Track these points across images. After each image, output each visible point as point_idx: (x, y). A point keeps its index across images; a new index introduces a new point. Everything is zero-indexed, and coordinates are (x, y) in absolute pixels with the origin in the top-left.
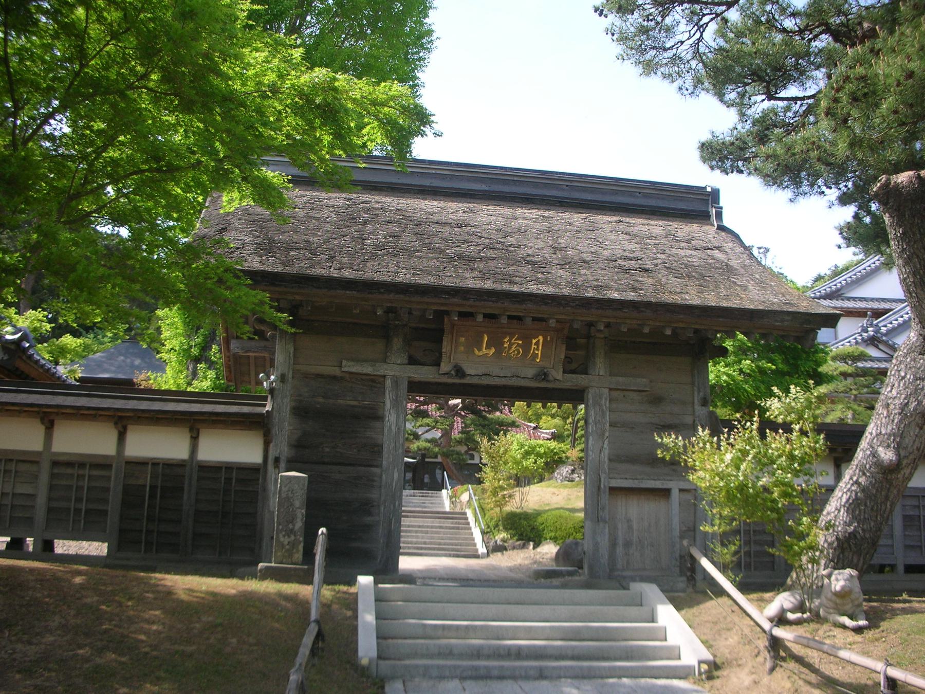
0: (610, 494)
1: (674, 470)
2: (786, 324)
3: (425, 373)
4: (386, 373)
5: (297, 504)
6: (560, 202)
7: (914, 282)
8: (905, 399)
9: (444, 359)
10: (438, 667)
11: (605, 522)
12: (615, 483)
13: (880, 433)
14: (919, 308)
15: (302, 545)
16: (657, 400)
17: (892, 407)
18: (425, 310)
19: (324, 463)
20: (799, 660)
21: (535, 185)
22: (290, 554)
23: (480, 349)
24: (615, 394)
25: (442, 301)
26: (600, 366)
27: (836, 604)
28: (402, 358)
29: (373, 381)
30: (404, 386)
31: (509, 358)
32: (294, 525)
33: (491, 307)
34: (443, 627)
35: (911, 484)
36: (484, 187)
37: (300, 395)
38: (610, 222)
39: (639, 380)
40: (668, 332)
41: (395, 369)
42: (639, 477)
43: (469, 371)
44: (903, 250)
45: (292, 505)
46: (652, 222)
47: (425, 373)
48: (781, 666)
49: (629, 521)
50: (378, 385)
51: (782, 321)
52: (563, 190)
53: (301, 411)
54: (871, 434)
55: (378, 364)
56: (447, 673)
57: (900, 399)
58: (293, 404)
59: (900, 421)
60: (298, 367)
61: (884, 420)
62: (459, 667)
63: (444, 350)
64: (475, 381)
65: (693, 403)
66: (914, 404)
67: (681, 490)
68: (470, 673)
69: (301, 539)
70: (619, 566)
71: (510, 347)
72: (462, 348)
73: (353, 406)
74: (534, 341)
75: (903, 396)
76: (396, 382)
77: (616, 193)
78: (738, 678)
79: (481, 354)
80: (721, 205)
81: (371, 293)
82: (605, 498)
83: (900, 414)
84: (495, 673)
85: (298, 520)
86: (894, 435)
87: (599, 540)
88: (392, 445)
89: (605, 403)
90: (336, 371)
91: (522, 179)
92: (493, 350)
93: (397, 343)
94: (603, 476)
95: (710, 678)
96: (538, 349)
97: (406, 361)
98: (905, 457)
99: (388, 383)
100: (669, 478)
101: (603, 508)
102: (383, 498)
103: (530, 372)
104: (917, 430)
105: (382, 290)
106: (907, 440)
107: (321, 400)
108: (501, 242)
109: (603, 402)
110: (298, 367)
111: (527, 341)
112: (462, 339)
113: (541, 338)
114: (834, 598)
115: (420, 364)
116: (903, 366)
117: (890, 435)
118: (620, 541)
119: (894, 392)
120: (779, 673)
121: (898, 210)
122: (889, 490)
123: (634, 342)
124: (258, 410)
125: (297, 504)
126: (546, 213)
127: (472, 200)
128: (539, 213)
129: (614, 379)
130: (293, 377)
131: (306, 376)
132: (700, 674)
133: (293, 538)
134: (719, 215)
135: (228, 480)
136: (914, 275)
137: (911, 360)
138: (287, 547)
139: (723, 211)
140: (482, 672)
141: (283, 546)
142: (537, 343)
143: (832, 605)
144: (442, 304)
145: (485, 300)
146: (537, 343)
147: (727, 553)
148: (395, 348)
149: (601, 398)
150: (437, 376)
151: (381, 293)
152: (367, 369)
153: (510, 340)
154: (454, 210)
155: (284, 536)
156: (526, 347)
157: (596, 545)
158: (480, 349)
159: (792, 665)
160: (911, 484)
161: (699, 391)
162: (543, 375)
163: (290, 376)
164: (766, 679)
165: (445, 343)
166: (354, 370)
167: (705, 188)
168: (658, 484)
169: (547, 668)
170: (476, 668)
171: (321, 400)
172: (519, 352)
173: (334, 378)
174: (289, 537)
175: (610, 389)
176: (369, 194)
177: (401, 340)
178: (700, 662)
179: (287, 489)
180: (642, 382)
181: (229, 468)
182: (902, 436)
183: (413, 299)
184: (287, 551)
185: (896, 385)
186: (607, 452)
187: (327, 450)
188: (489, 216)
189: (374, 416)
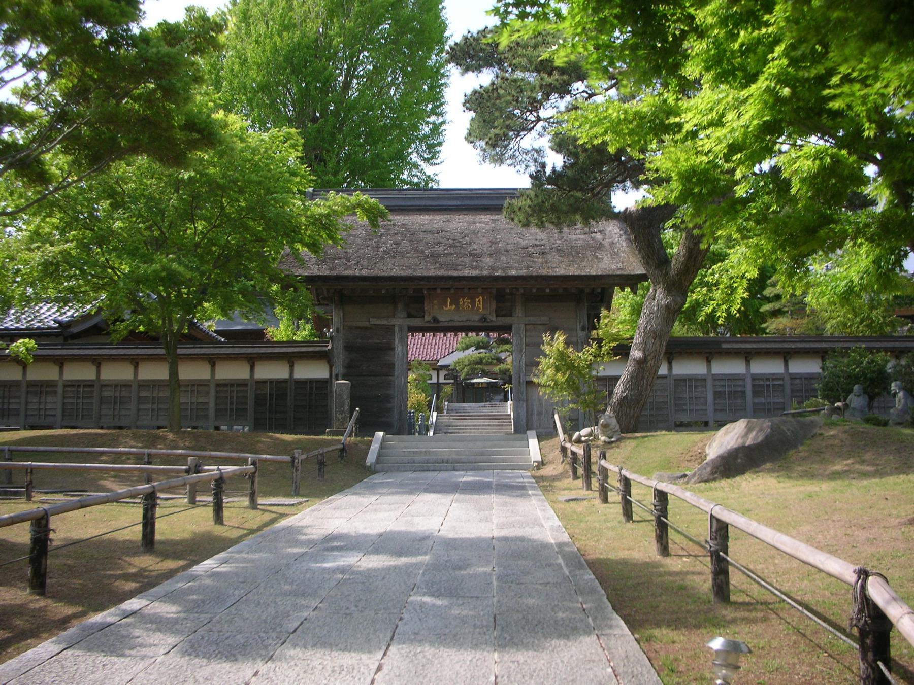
3: (416, 322)
5: (345, 397)
26: (519, 311)
36: (459, 203)
41: (399, 321)
47: (416, 322)
53: (349, 348)
64: (446, 324)
76: (401, 329)
90: (367, 324)
92: (454, 307)
93: (400, 306)
99: (396, 329)
103: (477, 318)
125: (345, 397)
126: (495, 217)
129: (528, 318)
135: (311, 388)
152: (384, 322)
162: (484, 319)
173: (366, 328)
180: (544, 319)
181: (311, 381)
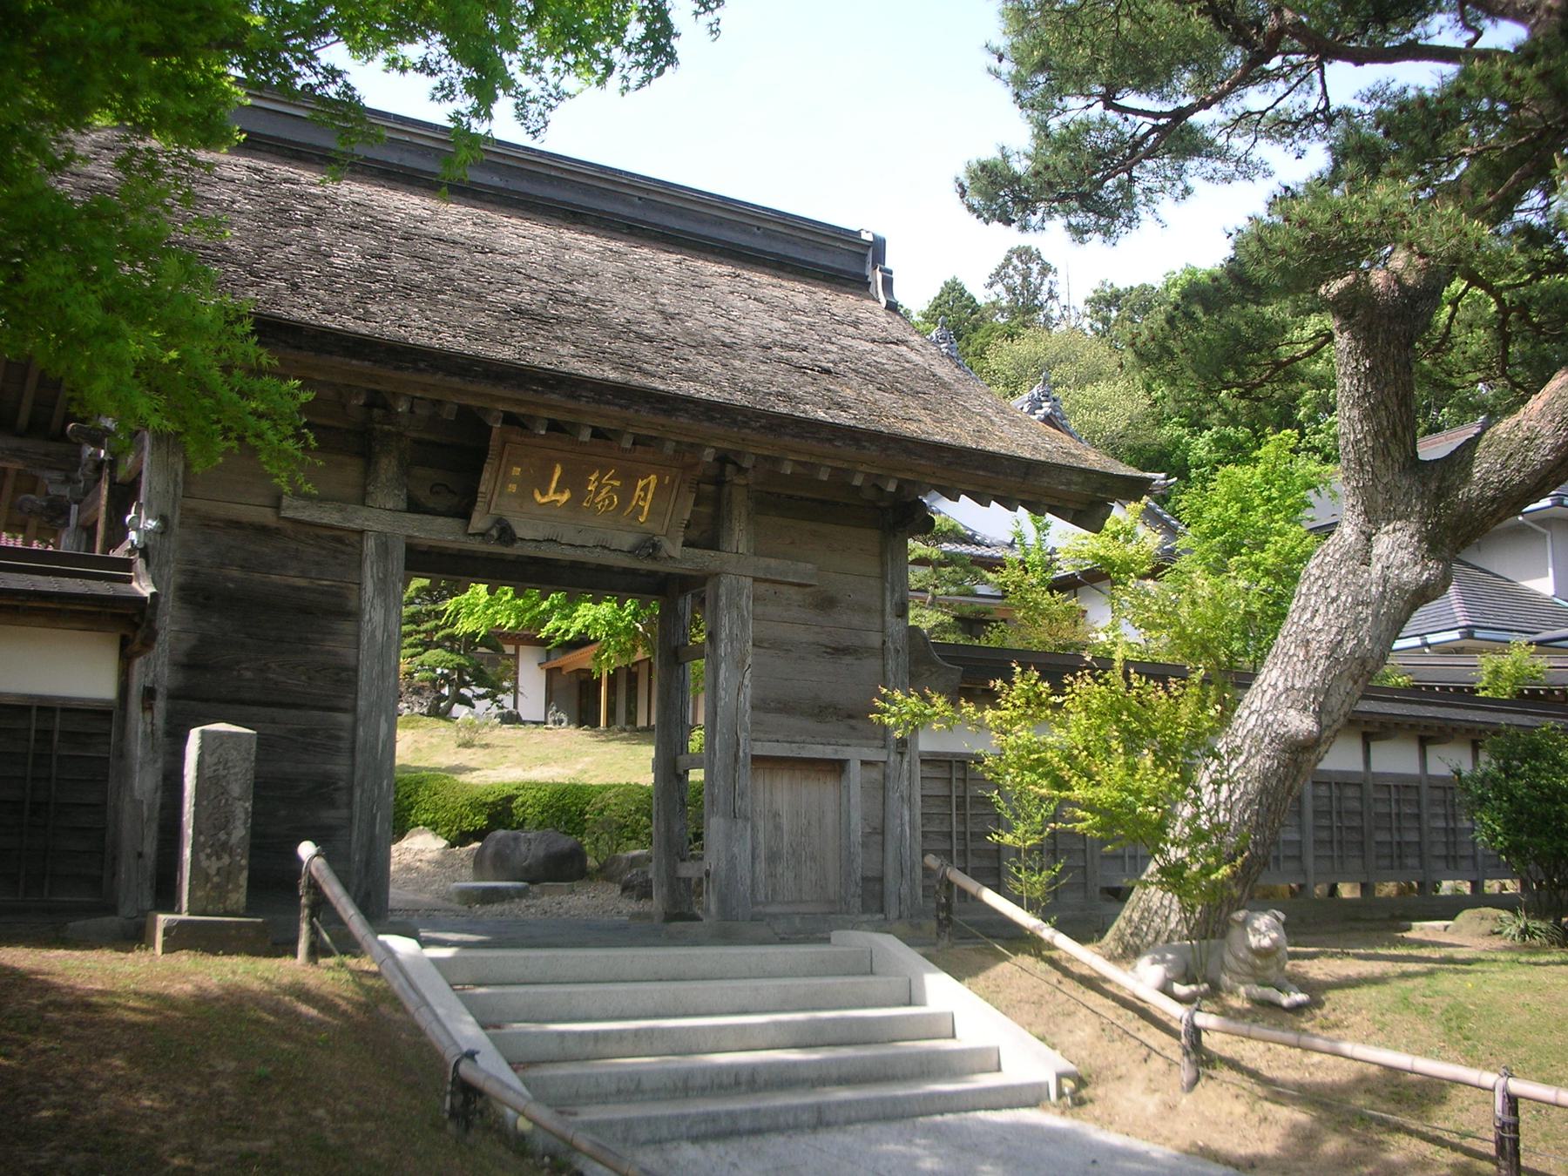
0: (754, 770)
1: (853, 728)
2: (1074, 488)
3: (439, 531)
4: (367, 525)
5: (236, 790)
6: (629, 227)
7: (1372, 448)
8: (1338, 633)
9: (480, 505)
10: (649, 1121)
11: (746, 818)
12: (763, 749)
13: (1293, 687)
14: (1371, 490)
15: (245, 874)
16: (826, 603)
17: (1314, 645)
18: (438, 403)
19: (243, 702)
20: (1234, 1065)
21: (587, 190)
22: (221, 891)
23: (544, 493)
24: (763, 587)
25: (529, 396)
26: (739, 537)
27: (1253, 966)
28: (396, 500)
29: (340, 540)
30: (399, 553)
31: (593, 508)
32: (229, 834)
33: (610, 415)
34: (596, 1034)
35: (1321, 766)
36: (495, 181)
37: (194, 562)
38: (721, 275)
39: (802, 565)
40: (891, 487)
41: (384, 520)
42: (798, 738)
43: (520, 533)
44: (1366, 394)
45: (225, 792)
46: (785, 283)
47: (439, 531)
48: (1211, 1077)
49: (776, 815)
50: (349, 549)
51: (1069, 483)
52: (633, 205)
53: (197, 594)
54: (1275, 686)
55: (350, 508)
56: (665, 1133)
57: (1329, 633)
58: (181, 579)
59: (1327, 670)
60: (191, 503)
61: (1299, 666)
62: (684, 1117)
63: (482, 489)
64: (530, 550)
65: (883, 611)
66: (1352, 643)
67: (863, 763)
68: (703, 1127)
69: (244, 862)
70: (761, 897)
71: (598, 492)
72: (513, 488)
73: (299, 588)
74: (641, 483)
75: (1334, 630)
76: (384, 549)
77: (720, 222)
78: (1128, 1100)
79: (545, 500)
80: (888, 265)
81: (397, 368)
82: (745, 775)
83: (1328, 658)
84: (746, 1123)
85: (238, 823)
86: (1316, 690)
87: (736, 850)
88: (377, 668)
89: (746, 603)
90: (267, 516)
91: (564, 176)
92: (566, 497)
93: (387, 467)
94: (742, 736)
95: (1080, 1102)
96: (644, 499)
97: (403, 505)
98: (1329, 727)
99: (370, 545)
100: (843, 741)
101: (742, 795)
102: (359, 774)
103: (627, 540)
104: (1351, 683)
105: (422, 365)
106: (1333, 700)
107: (236, 573)
108: (567, 292)
109: (743, 602)
110: (191, 503)
111: (629, 479)
112: (517, 471)
113: (653, 477)
114: (1250, 957)
115: (425, 513)
116: (1333, 581)
117: (1309, 691)
118: (762, 852)
119: (1318, 622)
120: (1206, 1089)
121: (1368, 329)
122: (1295, 780)
123: (791, 497)
124: (120, 589)
125: (236, 790)
126: (613, 245)
127: (478, 204)
128: (602, 242)
129: (764, 562)
130: (181, 524)
131: (207, 523)
132: (1060, 1095)
133: (226, 860)
134: (888, 284)
135: (45, 735)
136: (1376, 436)
137: (1348, 572)
138: (216, 879)
139: (894, 276)
140: (724, 1124)
141: (208, 878)
142: (645, 489)
143: (1246, 968)
144: (519, 402)
145: (608, 403)
146: (645, 489)
147: (1036, 882)
148: (383, 478)
149: (740, 595)
150: (462, 539)
151: (420, 371)
152: (330, 516)
153: (599, 479)
154: (455, 219)
155: (209, 857)
156: (626, 493)
157: (732, 860)
158: (544, 493)
159: (1226, 1074)
160: (1321, 766)
161: (893, 591)
162: (649, 547)
163: (176, 521)
164: (1185, 1100)
165: (486, 476)
166: (305, 515)
167: (859, 233)
168: (828, 752)
169: (829, 1105)
170: (713, 1118)
171: (236, 573)
172: (612, 502)
173: (262, 530)
174: (219, 858)
175: (755, 580)
176: (289, 164)
177: (394, 462)
178: (1060, 1077)
179: (214, 759)
180: (804, 570)
181: (46, 708)
182: (1327, 693)
183: (472, 388)
184: (217, 887)
185: (1322, 610)
186: (749, 691)
187: (248, 674)
188: (521, 237)
189: (338, 609)
